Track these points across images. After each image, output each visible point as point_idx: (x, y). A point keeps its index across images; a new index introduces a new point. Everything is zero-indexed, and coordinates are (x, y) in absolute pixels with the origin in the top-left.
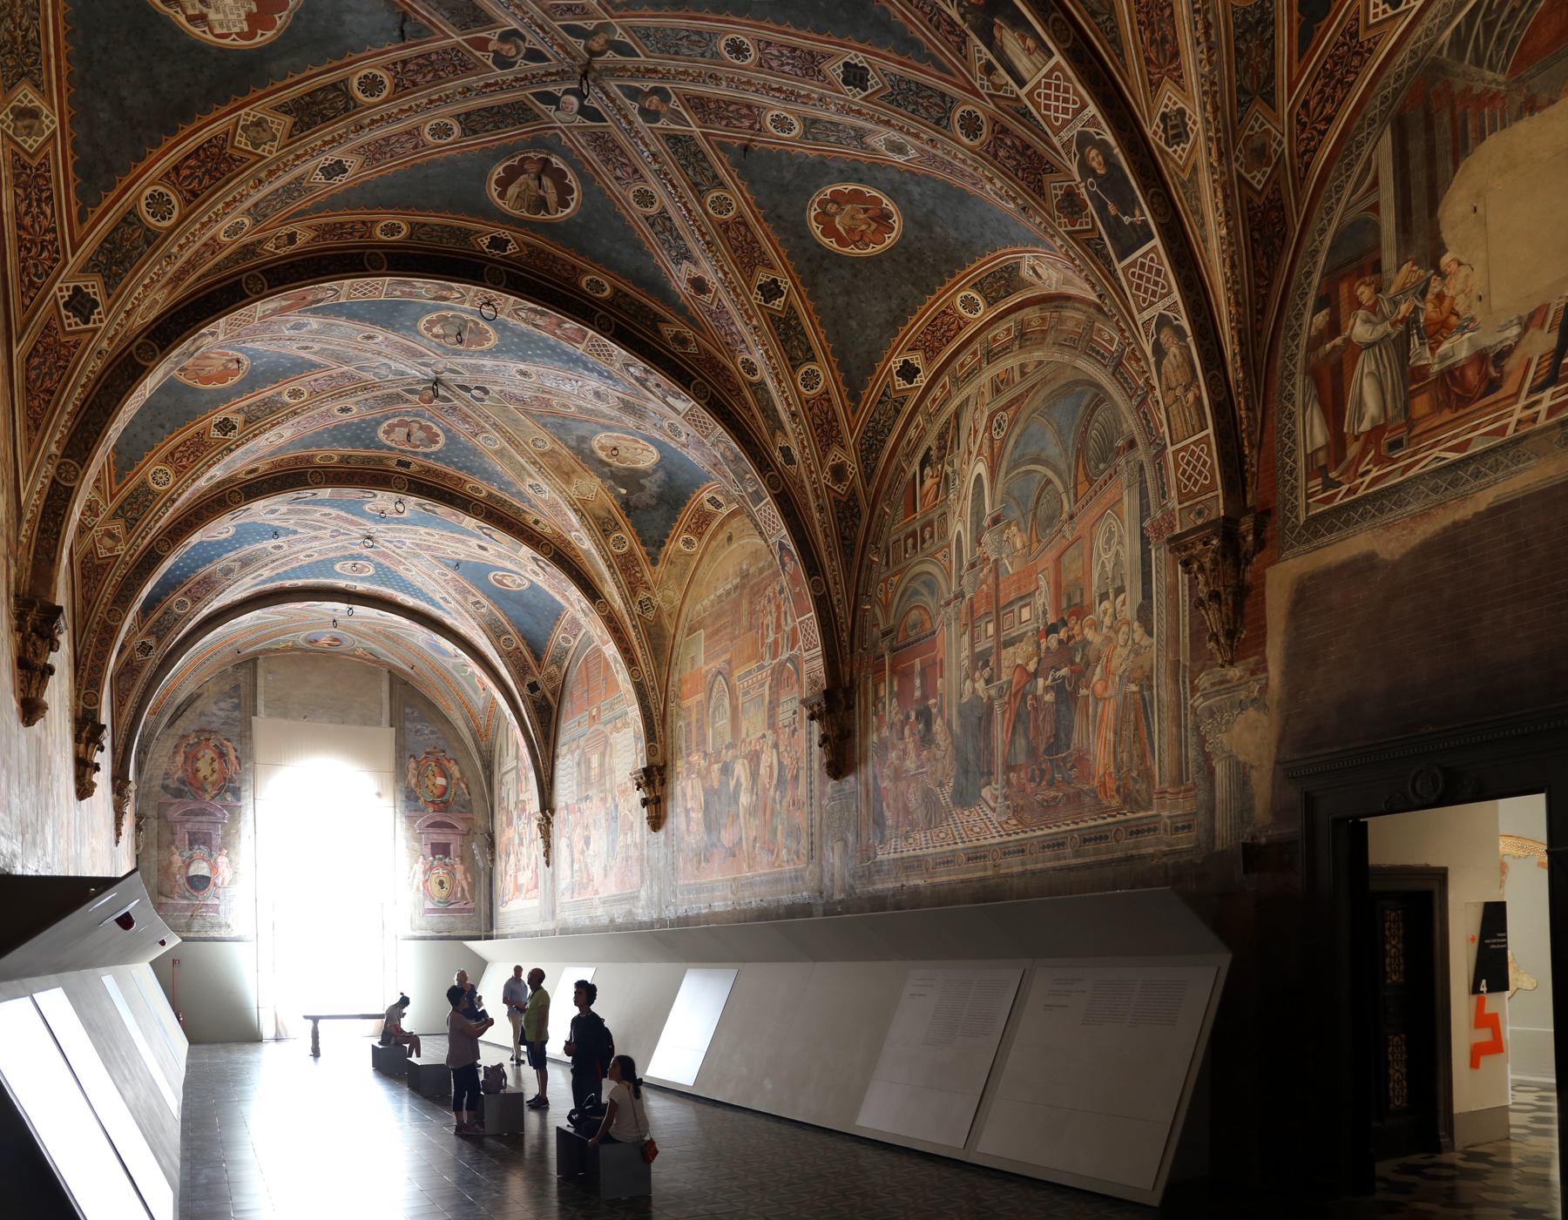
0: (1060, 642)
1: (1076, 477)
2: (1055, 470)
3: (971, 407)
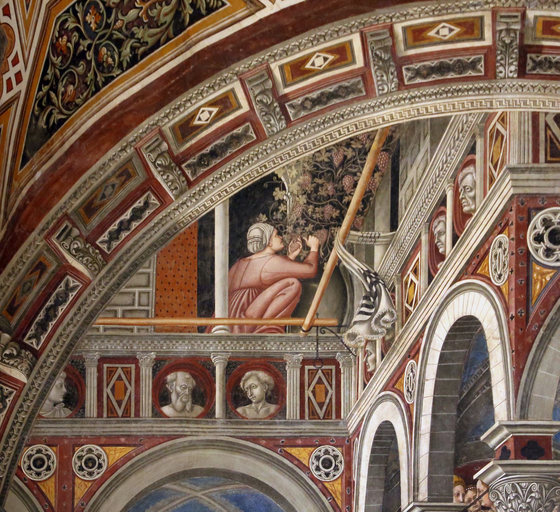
3: (450, 151)
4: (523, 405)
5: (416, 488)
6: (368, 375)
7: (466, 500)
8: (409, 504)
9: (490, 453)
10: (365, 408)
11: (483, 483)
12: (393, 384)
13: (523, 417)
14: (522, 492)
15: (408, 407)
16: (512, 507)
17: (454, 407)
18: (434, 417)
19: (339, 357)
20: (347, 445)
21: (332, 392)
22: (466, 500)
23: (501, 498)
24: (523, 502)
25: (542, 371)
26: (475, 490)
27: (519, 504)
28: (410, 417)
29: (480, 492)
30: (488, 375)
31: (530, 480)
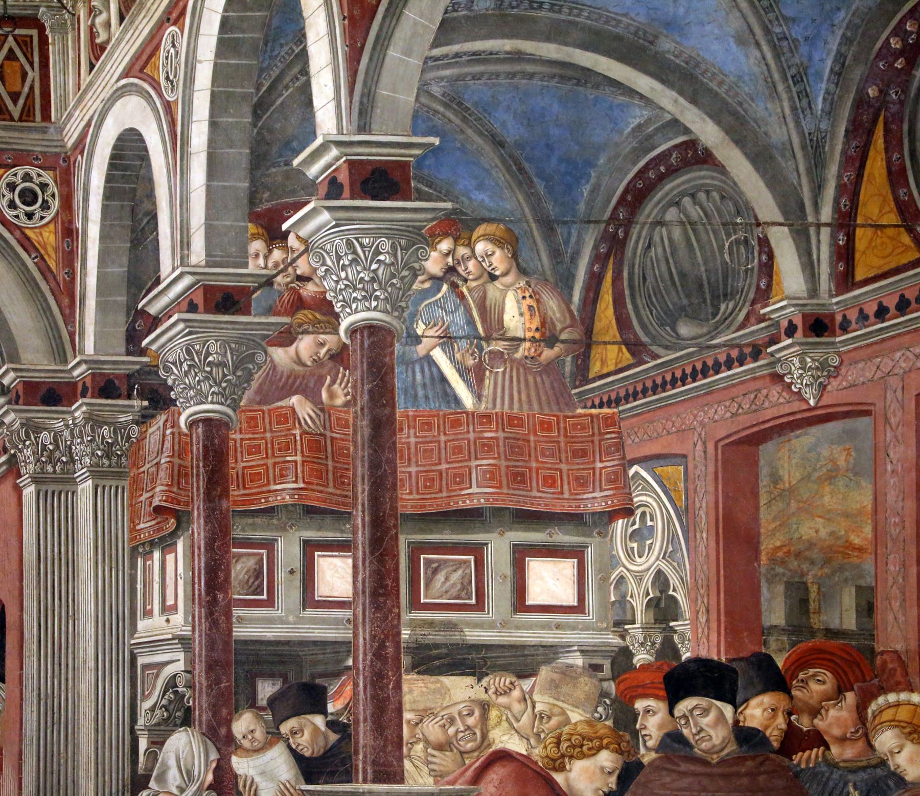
0: (746, 736)
1: (851, 192)
2: (739, 129)
4: (363, 108)
5: (186, 244)
6: (97, 50)
7: (270, 265)
8: (174, 270)
9: (310, 187)
10: (93, 105)
11: (298, 237)
12: (142, 64)
13: (363, 128)
14: (364, 252)
15: (168, 107)
16: (347, 278)
17: (247, 110)
18: (213, 125)
19: (43, 13)
20: (65, 167)
21: (33, 75)
22: (270, 265)
23: (329, 263)
24: (365, 269)
25: (393, 53)
26: (286, 249)
27: (359, 273)
28: (172, 123)
29: (293, 251)
30: (303, 56)
31: (376, 233)
